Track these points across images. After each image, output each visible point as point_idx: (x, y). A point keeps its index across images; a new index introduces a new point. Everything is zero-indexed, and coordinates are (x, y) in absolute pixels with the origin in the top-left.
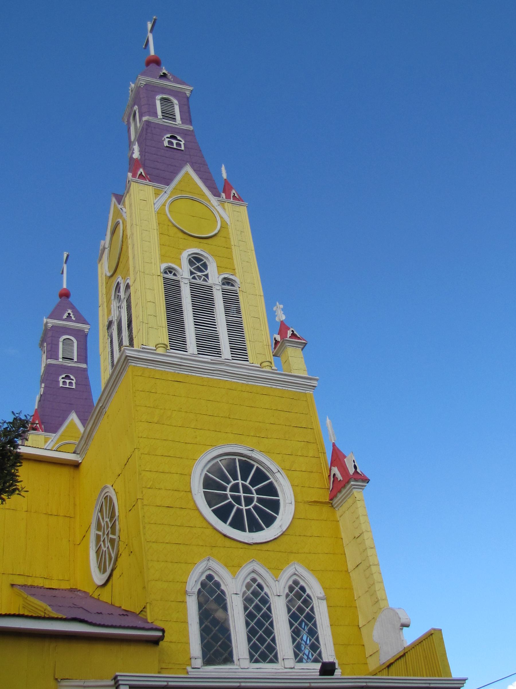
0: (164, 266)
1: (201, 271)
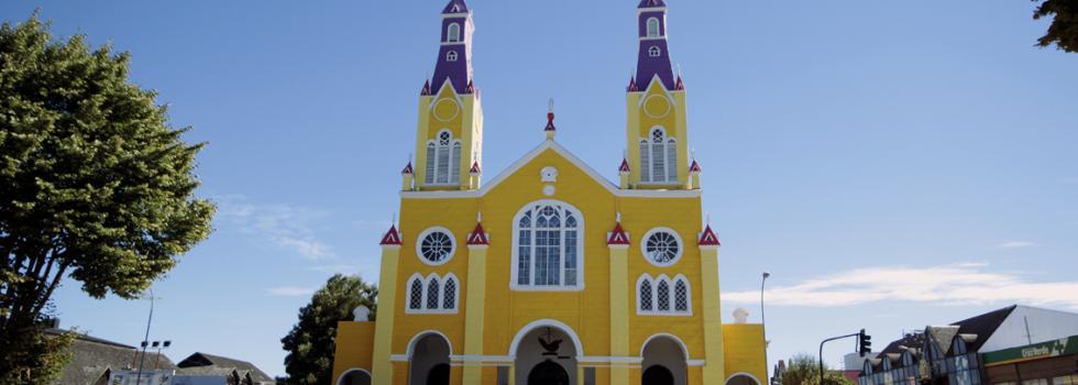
0: (641, 139)
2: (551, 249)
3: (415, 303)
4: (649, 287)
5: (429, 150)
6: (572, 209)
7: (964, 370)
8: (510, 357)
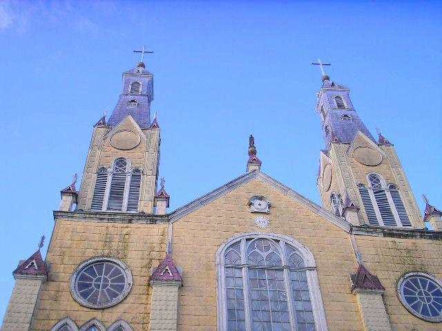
1: (377, 183)
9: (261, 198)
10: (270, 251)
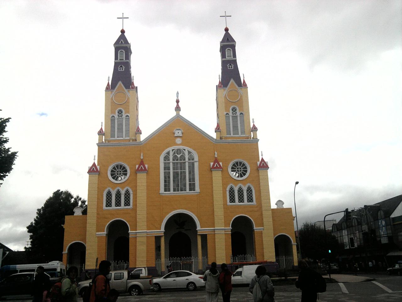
0: (225, 113)
2: (181, 173)
3: (109, 204)
4: (233, 191)
5: (111, 120)
6: (190, 150)
7: (383, 226)
8: (163, 229)
9: (179, 129)
10: (181, 154)
